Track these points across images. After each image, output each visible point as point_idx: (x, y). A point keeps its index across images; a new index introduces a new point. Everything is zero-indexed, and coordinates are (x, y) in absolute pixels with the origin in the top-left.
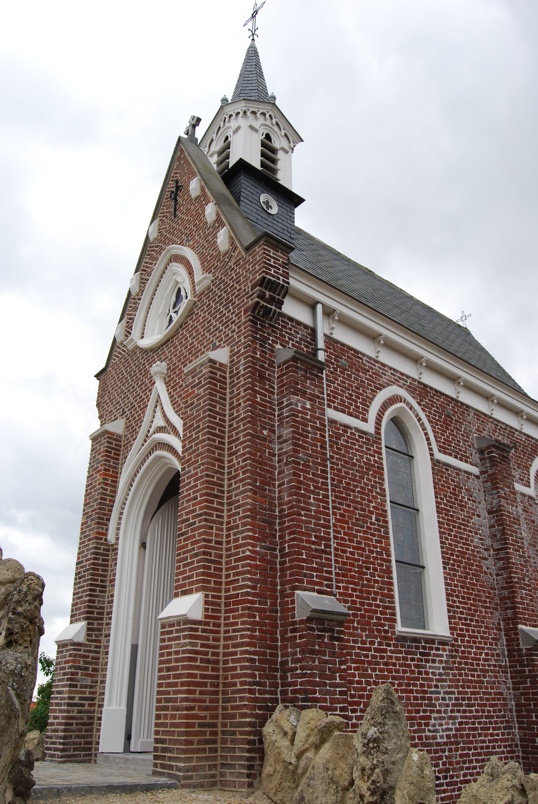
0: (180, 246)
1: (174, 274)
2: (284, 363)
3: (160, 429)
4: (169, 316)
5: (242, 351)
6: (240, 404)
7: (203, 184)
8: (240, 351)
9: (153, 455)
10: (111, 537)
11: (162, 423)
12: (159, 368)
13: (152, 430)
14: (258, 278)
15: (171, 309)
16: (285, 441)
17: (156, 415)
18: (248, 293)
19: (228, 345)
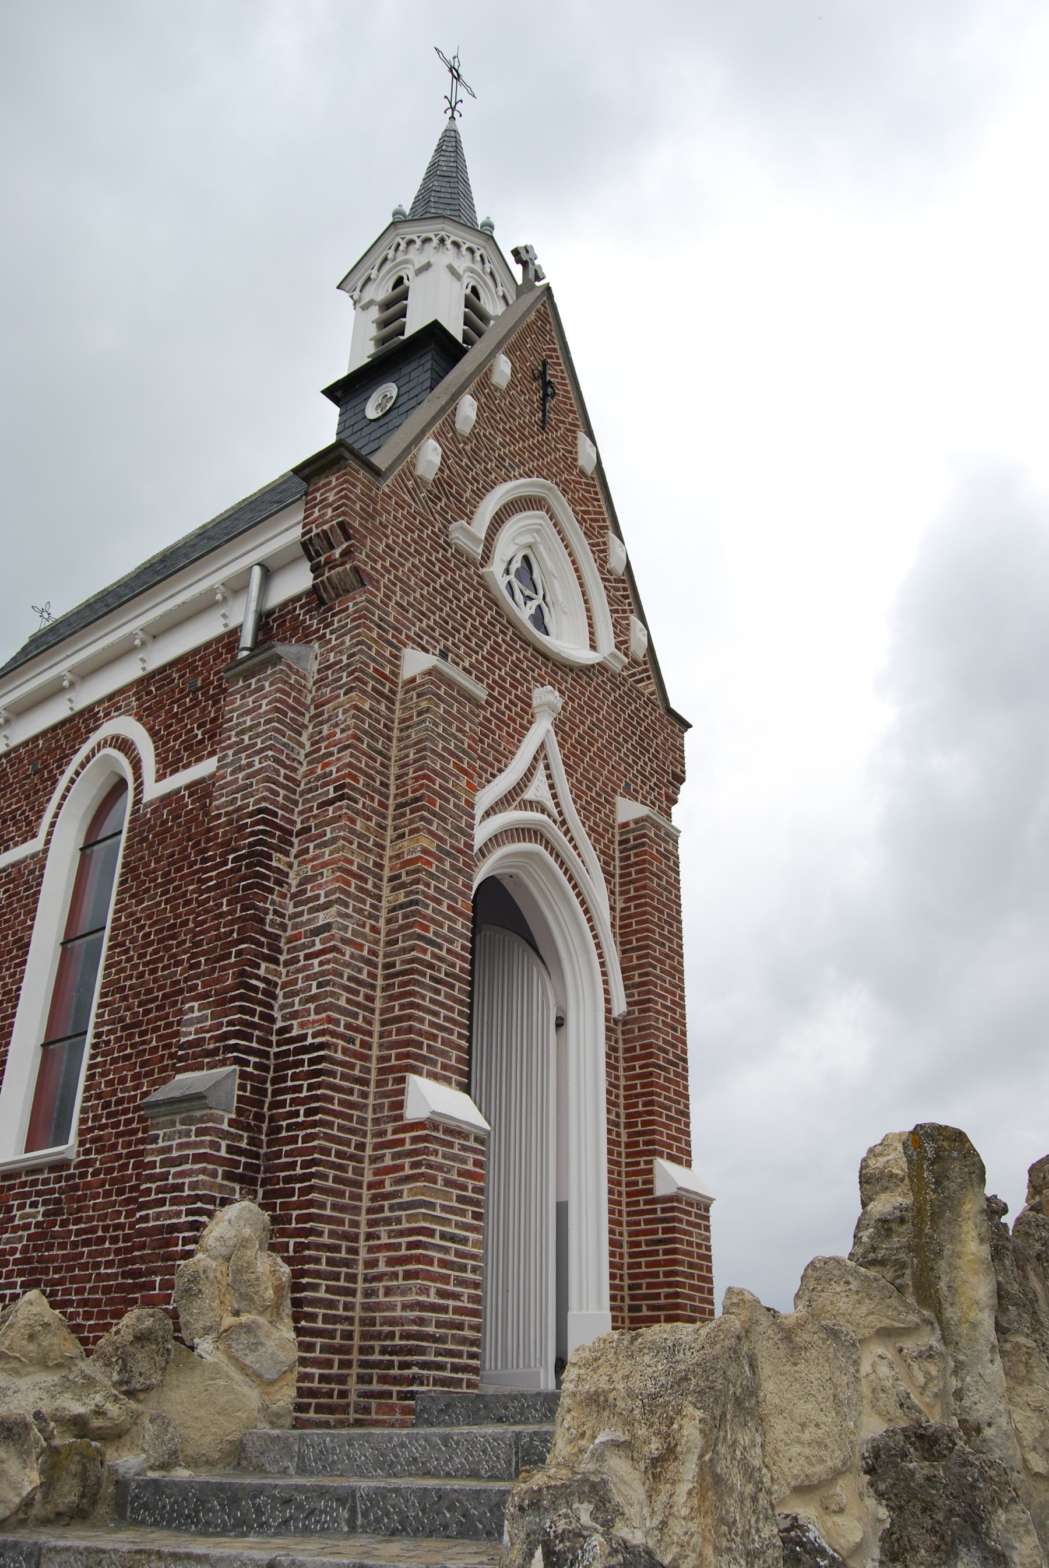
1: (538, 531)
3: (543, 811)
11: (529, 795)
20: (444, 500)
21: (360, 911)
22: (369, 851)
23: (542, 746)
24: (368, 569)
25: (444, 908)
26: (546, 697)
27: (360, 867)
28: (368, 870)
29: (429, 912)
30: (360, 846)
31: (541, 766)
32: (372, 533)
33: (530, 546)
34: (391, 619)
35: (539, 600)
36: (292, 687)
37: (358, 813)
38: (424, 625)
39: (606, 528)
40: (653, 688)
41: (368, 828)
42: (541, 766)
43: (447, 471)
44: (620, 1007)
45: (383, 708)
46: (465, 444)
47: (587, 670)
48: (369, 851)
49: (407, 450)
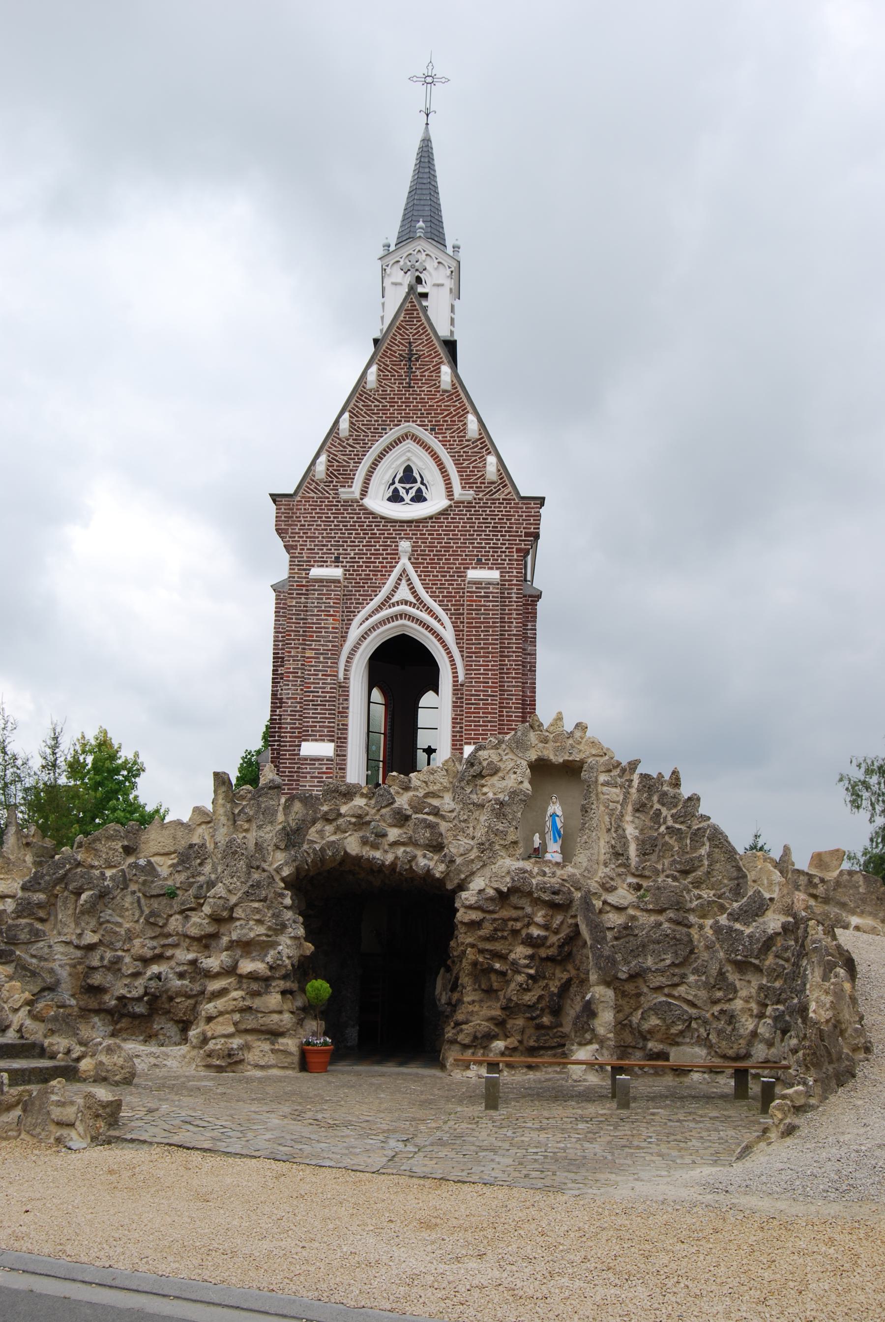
0: (420, 428)
1: (409, 451)
2: (530, 596)
3: (406, 602)
4: (392, 488)
5: (514, 582)
6: (512, 623)
7: (455, 381)
8: (511, 580)
9: (400, 622)
10: (341, 676)
12: (405, 546)
13: (394, 600)
14: (532, 530)
15: (397, 480)
16: (529, 654)
17: (401, 587)
18: (521, 536)
19: (497, 569)
20: (335, 479)
21: (295, 685)
22: (299, 661)
23: (404, 571)
24: (291, 543)
25: (320, 676)
26: (405, 546)
27: (294, 668)
28: (299, 668)
29: (312, 680)
30: (294, 661)
31: (404, 582)
32: (291, 525)
33: (409, 460)
34: (305, 559)
35: (418, 485)
36: (281, 599)
37: (292, 648)
38: (325, 551)
39: (468, 412)
40: (510, 489)
41: (298, 652)
42: (404, 582)
43: (336, 464)
44: (461, 678)
45: (303, 600)
46: (348, 440)
47: (444, 513)
48: (299, 661)
49: (309, 469)
